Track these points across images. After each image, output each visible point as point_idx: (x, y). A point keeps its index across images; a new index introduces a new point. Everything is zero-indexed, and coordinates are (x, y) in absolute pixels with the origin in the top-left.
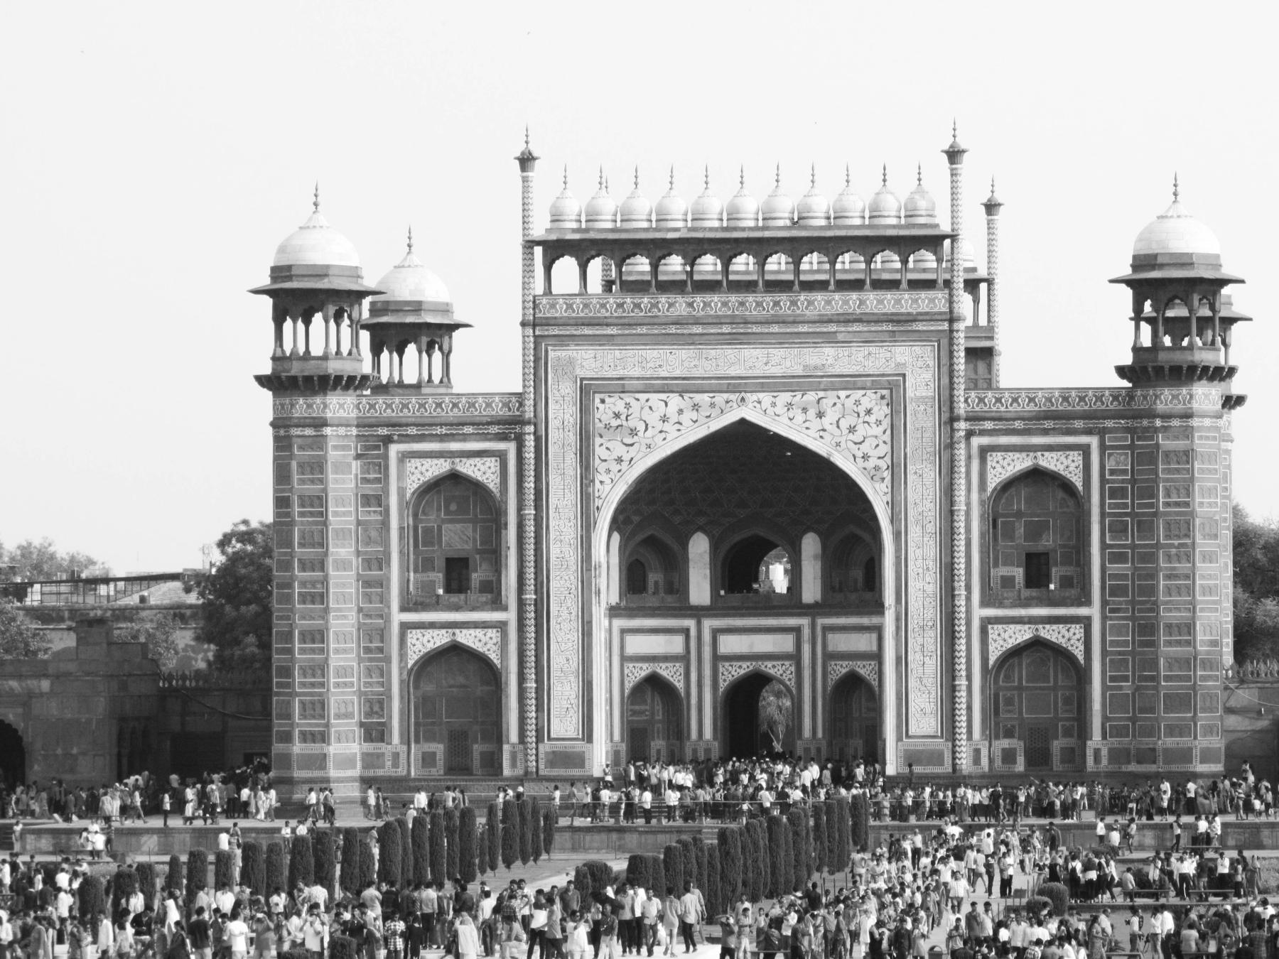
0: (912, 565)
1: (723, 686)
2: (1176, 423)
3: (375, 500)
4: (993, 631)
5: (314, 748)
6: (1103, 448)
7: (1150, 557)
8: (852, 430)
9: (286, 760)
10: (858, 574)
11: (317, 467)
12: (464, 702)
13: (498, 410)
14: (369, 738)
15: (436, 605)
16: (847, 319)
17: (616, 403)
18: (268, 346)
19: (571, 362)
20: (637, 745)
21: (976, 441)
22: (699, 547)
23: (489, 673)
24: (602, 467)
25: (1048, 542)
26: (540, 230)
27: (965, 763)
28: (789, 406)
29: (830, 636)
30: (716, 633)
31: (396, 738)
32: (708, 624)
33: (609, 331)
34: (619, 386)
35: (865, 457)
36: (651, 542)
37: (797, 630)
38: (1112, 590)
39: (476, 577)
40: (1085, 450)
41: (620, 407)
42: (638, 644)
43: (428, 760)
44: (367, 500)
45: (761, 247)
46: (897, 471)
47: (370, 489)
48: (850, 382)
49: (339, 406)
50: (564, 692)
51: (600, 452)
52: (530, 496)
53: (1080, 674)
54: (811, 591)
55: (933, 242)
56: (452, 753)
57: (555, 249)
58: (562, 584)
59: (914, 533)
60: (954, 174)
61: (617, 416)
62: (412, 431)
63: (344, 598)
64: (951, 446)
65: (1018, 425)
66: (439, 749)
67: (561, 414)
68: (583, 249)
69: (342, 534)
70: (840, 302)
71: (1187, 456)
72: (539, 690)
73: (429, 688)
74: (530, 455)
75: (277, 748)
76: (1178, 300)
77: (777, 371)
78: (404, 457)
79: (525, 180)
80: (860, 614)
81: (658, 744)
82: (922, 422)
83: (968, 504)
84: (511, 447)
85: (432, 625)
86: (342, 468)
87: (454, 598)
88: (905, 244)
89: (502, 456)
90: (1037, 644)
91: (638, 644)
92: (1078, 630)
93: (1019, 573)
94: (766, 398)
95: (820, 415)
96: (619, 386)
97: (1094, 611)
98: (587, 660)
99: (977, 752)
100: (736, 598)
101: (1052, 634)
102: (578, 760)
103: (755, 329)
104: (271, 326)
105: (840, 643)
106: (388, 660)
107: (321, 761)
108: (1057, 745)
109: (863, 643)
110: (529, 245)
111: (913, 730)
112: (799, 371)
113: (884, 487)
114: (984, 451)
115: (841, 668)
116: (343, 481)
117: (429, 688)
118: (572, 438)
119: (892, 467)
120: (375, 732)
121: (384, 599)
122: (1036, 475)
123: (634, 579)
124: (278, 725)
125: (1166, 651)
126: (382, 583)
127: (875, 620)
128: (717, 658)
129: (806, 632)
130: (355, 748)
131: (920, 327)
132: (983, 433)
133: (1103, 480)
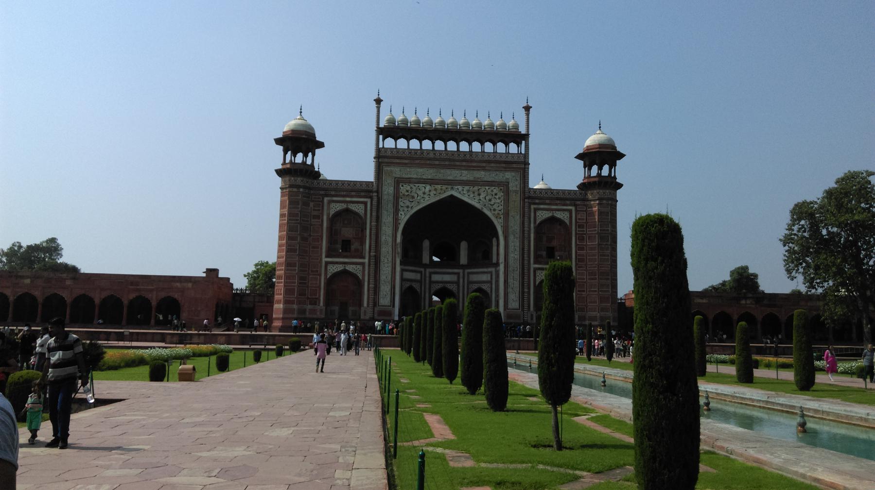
0: (508, 248)
1: (432, 292)
2: (604, 202)
4: (538, 273)
6: (576, 211)
8: (490, 200)
13: (364, 187)
14: (311, 304)
18: (282, 161)
19: (391, 171)
21: (533, 207)
22: (426, 244)
24: (401, 209)
25: (555, 243)
26: (381, 125)
28: (468, 191)
29: (471, 276)
30: (431, 273)
31: (322, 304)
32: (428, 270)
33: (406, 161)
34: (409, 181)
35: (494, 210)
37: (458, 274)
39: (353, 247)
41: (408, 188)
44: (316, 217)
46: (506, 215)
47: (316, 213)
48: (490, 184)
50: (385, 289)
51: (401, 204)
58: (386, 250)
59: (511, 238)
60: (528, 115)
61: (407, 191)
62: (333, 193)
64: (524, 208)
65: (547, 201)
67: (388, 190)
74: (375, 203)
75: (276, 306)
77: (465, 178)
78: (330, 202)
79: (378, 108)
80: (483, 267)
82: (515, 199)
83: (529, 228)
84: (369, 200)
87: (345, 254)
89: (365, 203)
91: (407, 275)
93: (544, 253)
94: (460, 188)
95: (479, 195)
96: (409, 181)
99: (532, 315)
102: (390, 314)
103: (458, 163)
104: (282, 153)
105: (474, 278)
106: (320, 275)
109: (485, 278)
111: (510, 306)
112: (472, 179)
118: (391, 198)
122: (553, 220)
124: (276, 297)
127: (490, 270)
128: (431, 282)
129: (461, 275)
131: (514, 166)
133: (576, 222)
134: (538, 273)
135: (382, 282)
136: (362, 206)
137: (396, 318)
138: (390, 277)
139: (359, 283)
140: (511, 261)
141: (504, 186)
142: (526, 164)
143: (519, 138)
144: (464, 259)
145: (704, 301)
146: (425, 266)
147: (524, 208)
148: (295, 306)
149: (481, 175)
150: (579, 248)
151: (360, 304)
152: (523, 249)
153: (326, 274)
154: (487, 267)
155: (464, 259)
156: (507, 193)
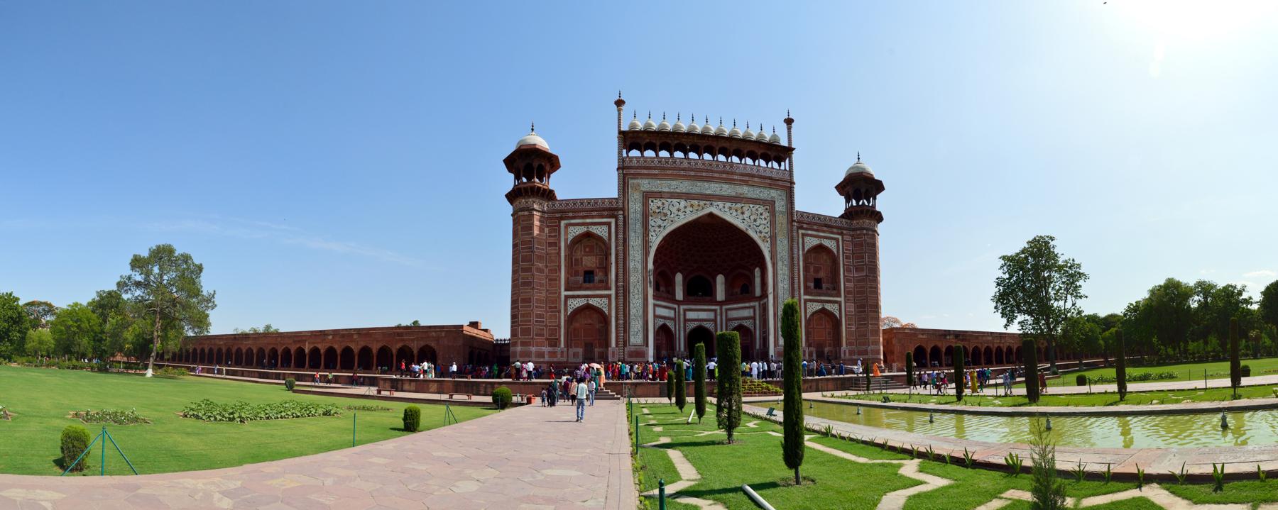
13: (607, 205)
15: (580, 289)
17: (658, 203)
22: (679, 278)
30: (685, 311)
32: (682, 307)
37: (715, 311)
41: (660, 204)
42: (661, 312)
44: (551, 244)
46: (773, 238)
47: (552, 240)
50: (636, 325)
51: (651, 223)
52: (621, 241)
56: (586, 352)
58: (635, 280)
59: (780, 264)
60: (789, 129)
63: (542, 285)
64: (792, 231)
66: (580, 350)
67: (635, 207)
69: (540, 258)
72: (625, 324)
73: (577, 325)
74: (621, 223)
78: (567, 226)
82: (782, 220)
84: (613, 221)
85: (579, 296)
87: (587, 285)
90: (823, 311)
91: (661, 312)
92: (837, 306)
94: (721, 204)
100: (692, 298)
108: (826, 350)
109: (746, 313)
113: (768, 245)
118: (639, 216)
128: (686, 320)
132: (802, 228)
134: (809, 304)
135: (632, 317)
136: (605, 228)
137: (651, 360)
139: (605, 319)
140: (780, 292)
141: (770, 204)
143: (780, 153)
144: (720, 294)
146: (679, 303)
148: (533, 349)
149: (745, 191)
151: (607, 343)
152: (793, 279)
153: (566, 310)
154: (750, 300)
155: (720, 294)
156: (773, 213)
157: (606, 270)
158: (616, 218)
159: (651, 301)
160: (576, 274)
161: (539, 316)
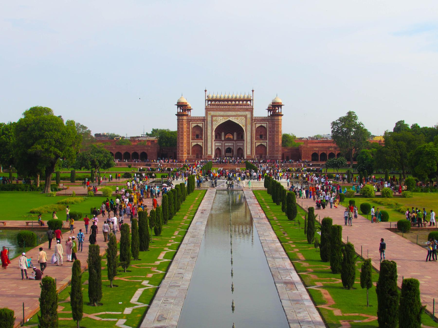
0: (247, 136)
3: (188, 128)
5: (182, 155)
7: (274, 135)
9: (179, 157)
10: (240, 137)
11: (182, 124)
12: (198, 151)
13: (202, 118)
15: (195, 140)
16: (241, 109)
17: (215, 118)
20: (216, 156)
22: (223, 134)
23: (201, 147)
25: (262, 133)
27: (253, 157)
34: (216, 116)
36: (218, 133)
38: (269, 139)
39: (199, 137)
40: (267, 124)
42: (217, 144)
43: (194, 157)
45: (231, 101)
48: (241, 116)
49: (185, 118)
50: (209, 149)
53: (266, 148)
54: (235, 139)
55: (250, 101)
57: (208, 101)
59: (248, 132)
64: (252, 123)
66: (195, 155)
67: (209, 119)
68: (211, 101)
69: (185, 132)
70: (240, 107)
71: (278, 124)
75: (177, 155)
76: (275, 108)
78: (192, 123)
81: (218, 155)
82: (249, 120)
86: (185, 124)
88: (247, 101)
90: (261, 145)
91: (217, 144)
92: (266, 143)
93: (259, 137)
96: (216, 116)
97: (267, 141)
98: (211, 146)
101: (263, 143)
102: (211, 157)
105: (238, 144)
107: (183, 157)
108: (263, 156)
109: (242, 144)
110: (206, 100)
114: (256, 123)
115: (239, 147)
116: (185, 126)
117: (194, 149)
118: (210, 122)
119: (246, 125)
120: (188, 154)
121: (189, 139)
122: (261, 126)
123: (216, 137)
124: (178, 153)
125: (276, 145)
126: (189, 137)
128: (225, 146)
130: (186, 155)
136: (202, 124)
138: (211, 146)
141: (246, 116)
142: (252, 109)
145: (317, 149)
146: (223, 141)
147: (252, 123)
149: (239, 113)
150: (269, 135)
157: (202, 135)
158: (205, 122)
159: (213, 143)
160: (194, 135)
161: (185, 147)
